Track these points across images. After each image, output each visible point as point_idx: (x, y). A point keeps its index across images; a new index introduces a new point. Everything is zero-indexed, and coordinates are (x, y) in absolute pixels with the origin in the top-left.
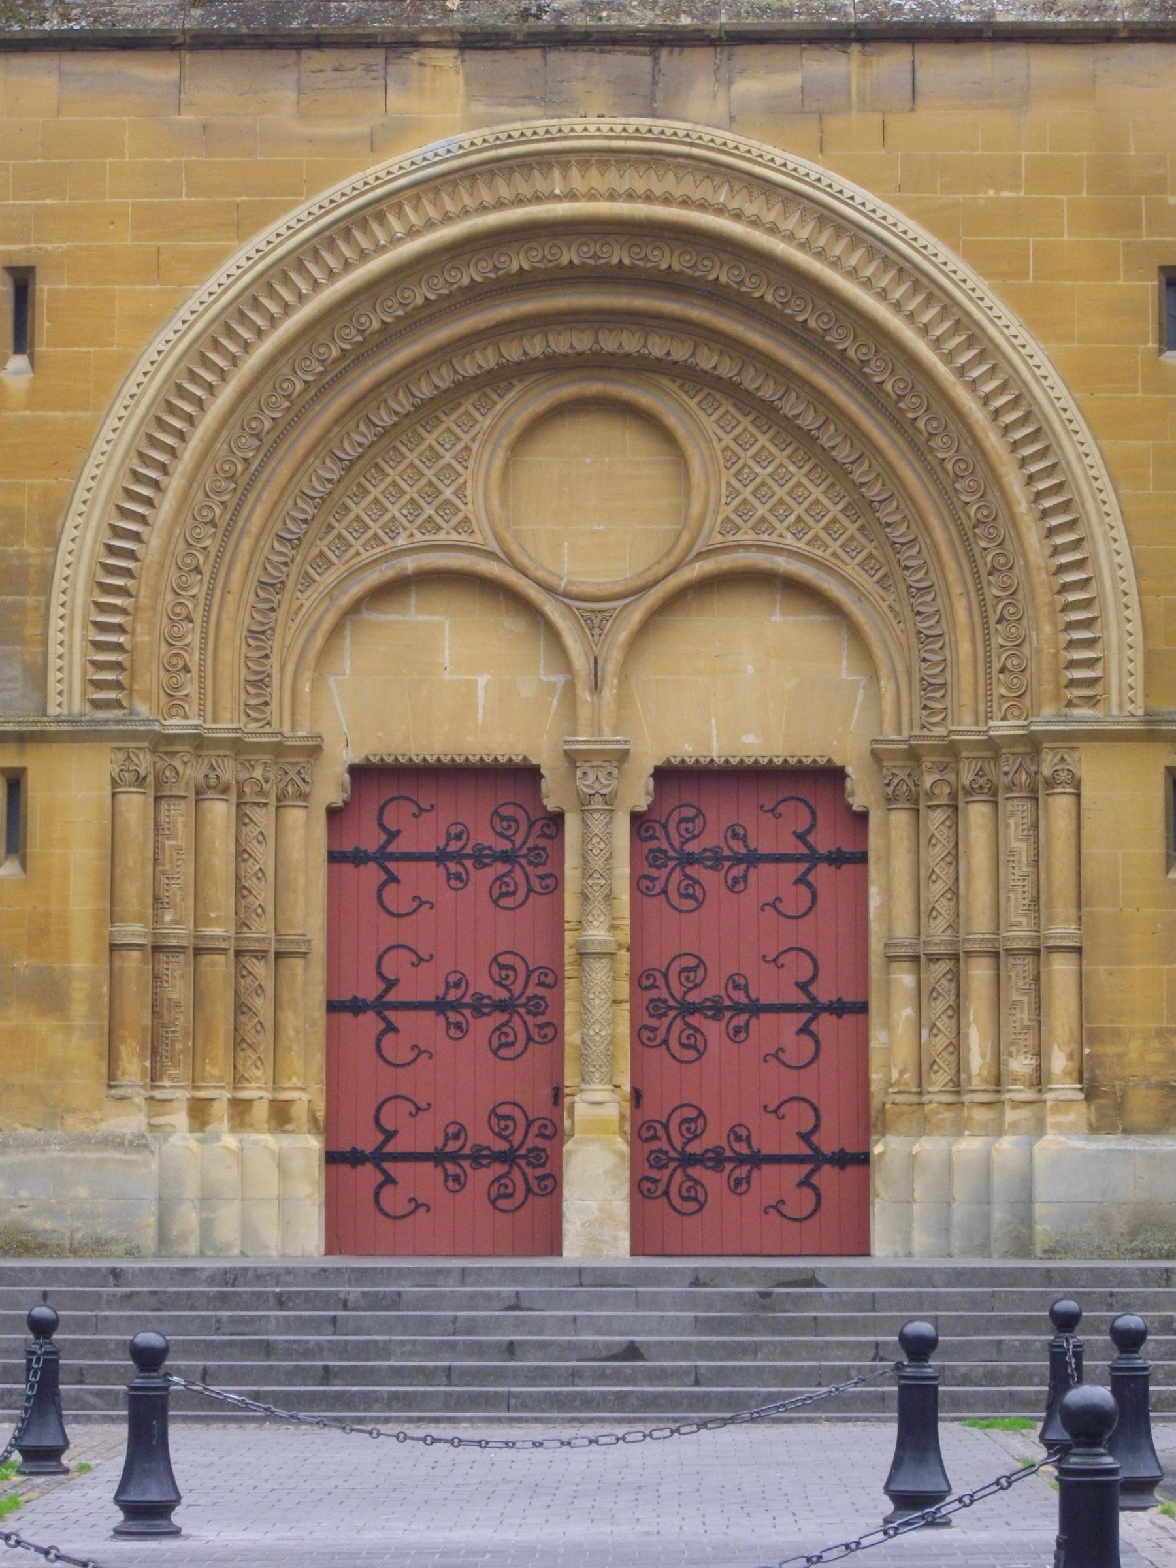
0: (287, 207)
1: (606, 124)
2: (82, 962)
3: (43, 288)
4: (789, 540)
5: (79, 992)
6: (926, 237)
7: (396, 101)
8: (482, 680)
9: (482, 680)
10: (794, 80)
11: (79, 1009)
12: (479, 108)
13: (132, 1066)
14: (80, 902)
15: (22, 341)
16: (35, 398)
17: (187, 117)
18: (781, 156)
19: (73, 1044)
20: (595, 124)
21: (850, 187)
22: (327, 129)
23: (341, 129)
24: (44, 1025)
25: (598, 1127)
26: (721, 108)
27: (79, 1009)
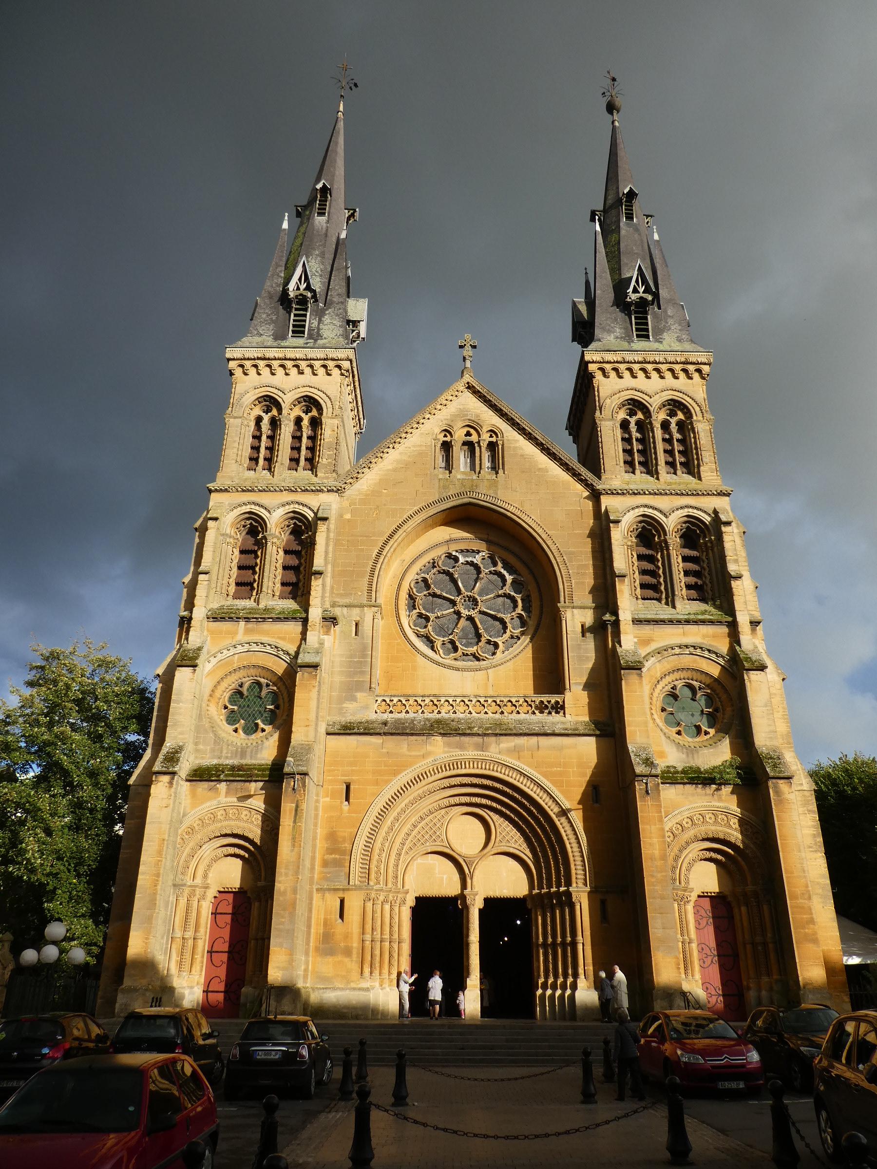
0: (405, 770)
1: (473, 753)
2: (355, 944)
3: (352, 787)
4: (513, 845)
5: (355, 952)
6: (542, 778)
7: (429, 748)
8: (445, 877)
9: (445, 877)
10: (513, 744)
11: (354, 956)
12: (446, 749)
13: (367, 970)
14: (356, 929)
15: (347, 799)
16: (349, 812)
17: (384, 750)
18: (508, 759)
19: (352, 964)
20: (471, 753)
21: (526, 767)
22: (413, 753)
23: (418, 753)
24: (346, 960)
25: (474, 986)
26: (497, 750)
27: (354, 956)
